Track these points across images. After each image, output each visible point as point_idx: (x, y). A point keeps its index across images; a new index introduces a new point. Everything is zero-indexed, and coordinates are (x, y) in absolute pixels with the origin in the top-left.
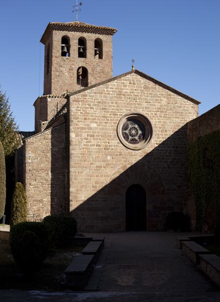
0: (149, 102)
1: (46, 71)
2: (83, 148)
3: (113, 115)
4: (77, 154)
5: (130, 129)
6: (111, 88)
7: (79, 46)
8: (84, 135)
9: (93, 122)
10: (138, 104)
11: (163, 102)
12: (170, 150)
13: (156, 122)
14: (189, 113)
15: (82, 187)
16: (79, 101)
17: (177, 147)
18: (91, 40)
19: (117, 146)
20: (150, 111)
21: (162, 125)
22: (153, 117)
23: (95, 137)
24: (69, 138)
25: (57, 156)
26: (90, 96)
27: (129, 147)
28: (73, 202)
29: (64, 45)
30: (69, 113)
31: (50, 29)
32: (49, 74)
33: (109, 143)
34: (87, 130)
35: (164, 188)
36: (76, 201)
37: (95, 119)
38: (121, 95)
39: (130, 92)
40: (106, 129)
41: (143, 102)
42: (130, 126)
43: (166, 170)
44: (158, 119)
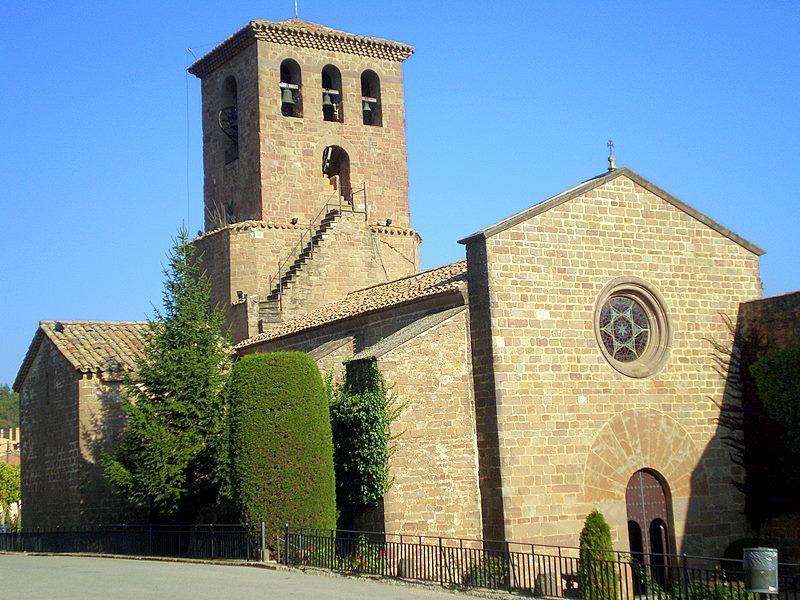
0: (657, 253)
2: (524, 376)
6: (573, 217)
8: (525, 342)
10: (635, 258)
12: (710, 376)
14: (742, 279)
15: (529, 481)
18: (351, 74)
19: (597, 367)
20: (660, 276)
21: (688, 311)
28: (512, 526)
34: (529, 327)
35: (705, 476)
37: (544, 298)
38: (595, 233)
40: (572, 325)
41: (644, 252)
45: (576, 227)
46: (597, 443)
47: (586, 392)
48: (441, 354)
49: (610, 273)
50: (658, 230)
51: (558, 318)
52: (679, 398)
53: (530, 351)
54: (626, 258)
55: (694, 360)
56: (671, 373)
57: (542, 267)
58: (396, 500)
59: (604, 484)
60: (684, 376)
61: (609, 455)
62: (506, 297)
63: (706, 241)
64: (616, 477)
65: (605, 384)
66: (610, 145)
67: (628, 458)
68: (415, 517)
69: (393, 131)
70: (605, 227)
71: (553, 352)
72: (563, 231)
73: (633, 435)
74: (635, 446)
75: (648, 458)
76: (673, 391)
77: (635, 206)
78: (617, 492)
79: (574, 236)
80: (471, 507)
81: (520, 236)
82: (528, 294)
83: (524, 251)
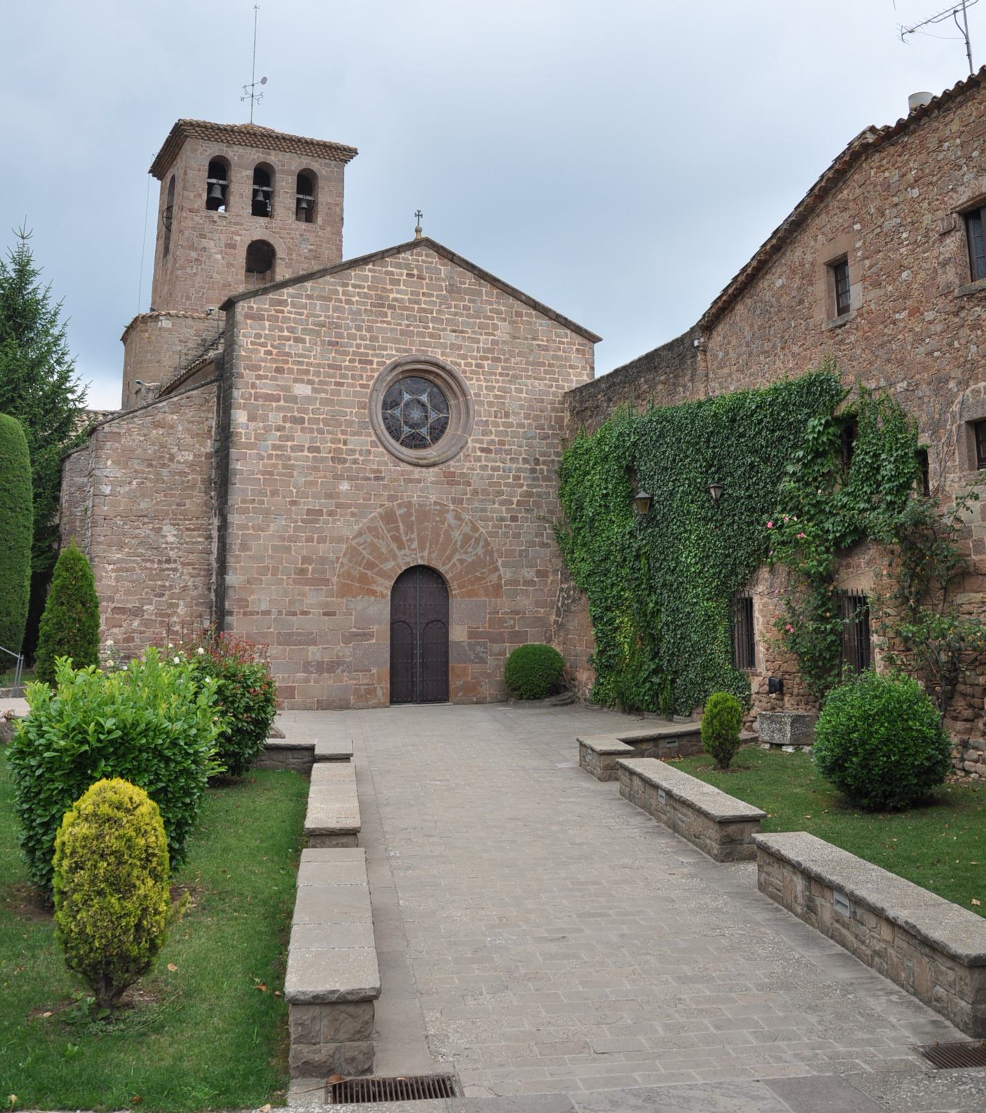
0: (462, 332)
1: (162, 249)
3: (361, 362)
4: (252, 472)
5: (407, 405)
6: (354, 286)
7: (257, 187)
8: (275, 418)
9: (302, 381)
10: (432, 336)
11: (498, 333)
12: (518, 470)
13: (480, 387)
14: (571, 367)
15: (264, 571)
16: (261, 318)
17: (537, 462)
18: (290, 172)
20: (464, 357)
21: (496, 397)
22: (472, 372)
23: (306, 425)
24: (229, 425)
25: (190, 477)
26: (293, 305)
27: (402, 456)
29: (214, 181)
30: (233, 351)
31: (180, 134)
32: (170, 257)
33: (345, 444)
34: (282, 403)
35: (500, 577)
36: (245, 614)
38: (382, 306)
39: (410, 301)
40: (340, 403)
41: (444, 330)
42: (407, 397)
43: (506, 526)
44: (486, 380)
45: (357, 298)
46: (360, 534)
47: (349, 479)
48: (180, 428)
49: (397, 350)
50: (466, 308)
51: (323, 395)
52: (475, 492)
53: (279, 429)
54: (421, 334)
55: (498, 452)
56: (467, 464)
57: (308, 338)
58: (105, 582)
59: (363, 579)
60: (484, 468)
61: (374, 549)
62: (256, 368)
63: (530, 323)
64: (382, 574)
65: (379, 471)
66: (419, 215)
67: (399, 554)
68: (128, 601)
69: (329, 229)
70: (395, 300)
71: (311, 430)
72: (340, 301)
73: (409, 527)
74: (411, 540)
75: (426, 554)
76: (469, 484)
77: (438, 279)
78: (379, 589)
79: (354, 307)
80: (201, 596)
81: (284, 303)
82: (286, 366)
83: (286, 320)
